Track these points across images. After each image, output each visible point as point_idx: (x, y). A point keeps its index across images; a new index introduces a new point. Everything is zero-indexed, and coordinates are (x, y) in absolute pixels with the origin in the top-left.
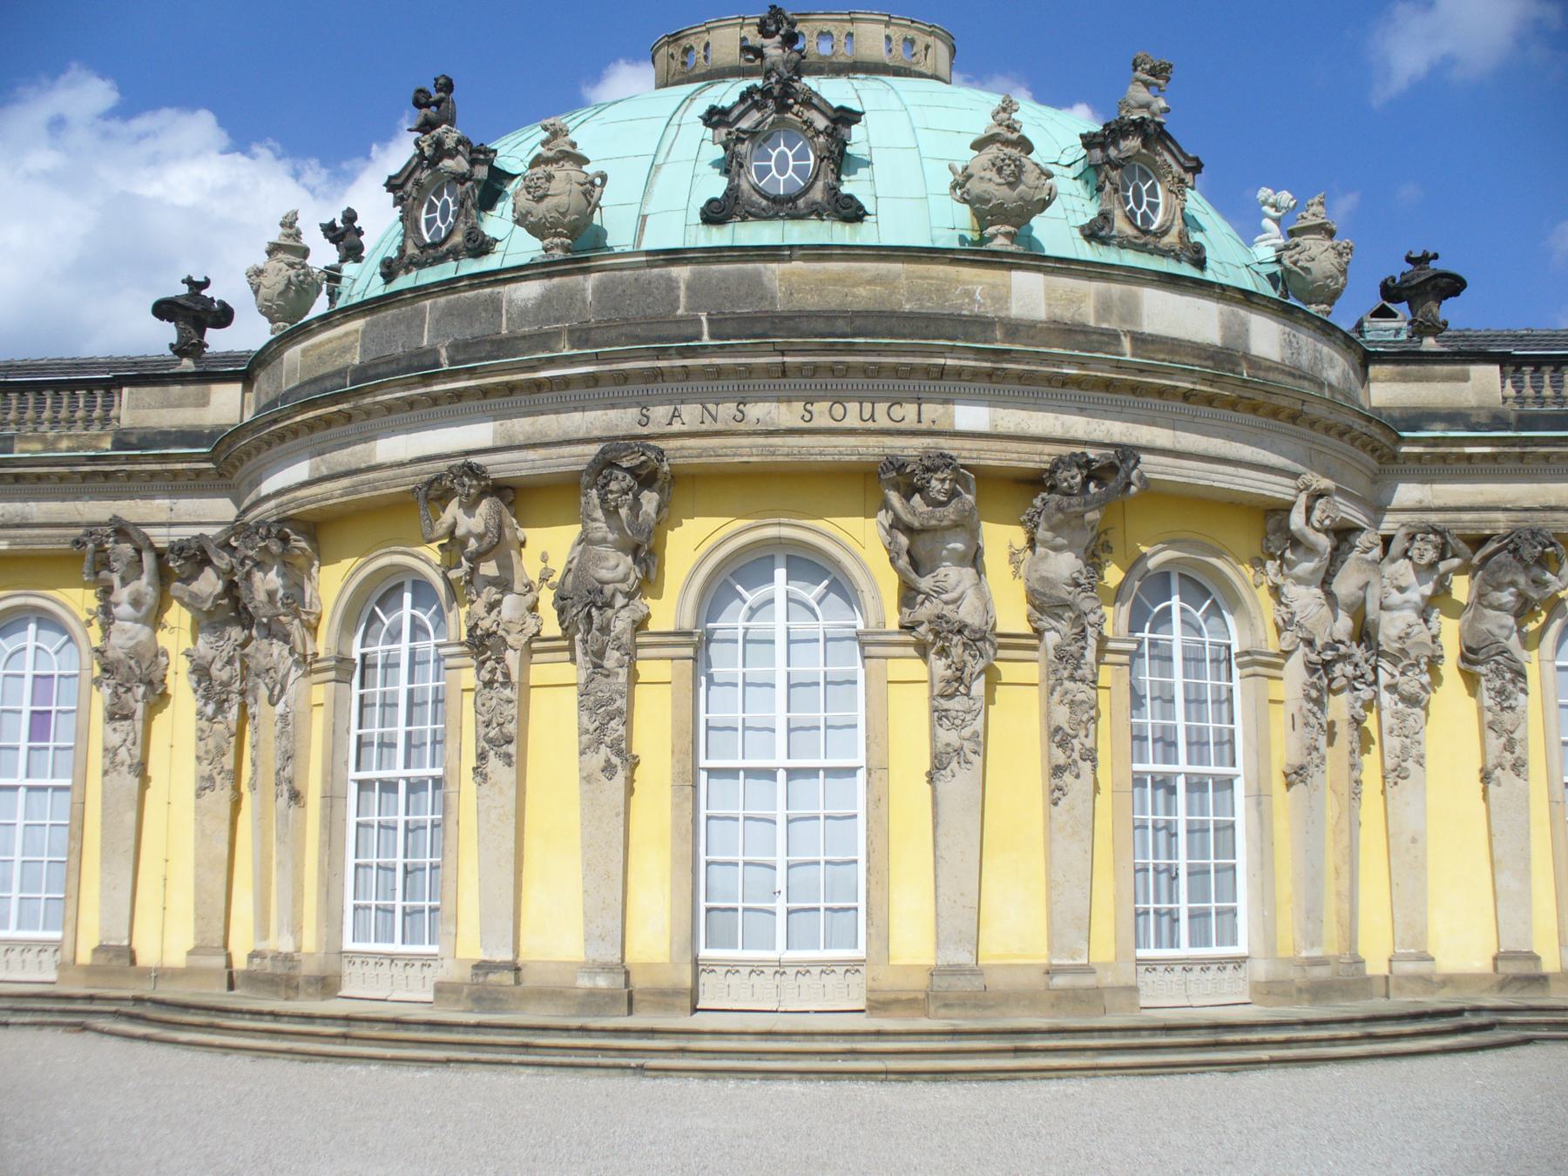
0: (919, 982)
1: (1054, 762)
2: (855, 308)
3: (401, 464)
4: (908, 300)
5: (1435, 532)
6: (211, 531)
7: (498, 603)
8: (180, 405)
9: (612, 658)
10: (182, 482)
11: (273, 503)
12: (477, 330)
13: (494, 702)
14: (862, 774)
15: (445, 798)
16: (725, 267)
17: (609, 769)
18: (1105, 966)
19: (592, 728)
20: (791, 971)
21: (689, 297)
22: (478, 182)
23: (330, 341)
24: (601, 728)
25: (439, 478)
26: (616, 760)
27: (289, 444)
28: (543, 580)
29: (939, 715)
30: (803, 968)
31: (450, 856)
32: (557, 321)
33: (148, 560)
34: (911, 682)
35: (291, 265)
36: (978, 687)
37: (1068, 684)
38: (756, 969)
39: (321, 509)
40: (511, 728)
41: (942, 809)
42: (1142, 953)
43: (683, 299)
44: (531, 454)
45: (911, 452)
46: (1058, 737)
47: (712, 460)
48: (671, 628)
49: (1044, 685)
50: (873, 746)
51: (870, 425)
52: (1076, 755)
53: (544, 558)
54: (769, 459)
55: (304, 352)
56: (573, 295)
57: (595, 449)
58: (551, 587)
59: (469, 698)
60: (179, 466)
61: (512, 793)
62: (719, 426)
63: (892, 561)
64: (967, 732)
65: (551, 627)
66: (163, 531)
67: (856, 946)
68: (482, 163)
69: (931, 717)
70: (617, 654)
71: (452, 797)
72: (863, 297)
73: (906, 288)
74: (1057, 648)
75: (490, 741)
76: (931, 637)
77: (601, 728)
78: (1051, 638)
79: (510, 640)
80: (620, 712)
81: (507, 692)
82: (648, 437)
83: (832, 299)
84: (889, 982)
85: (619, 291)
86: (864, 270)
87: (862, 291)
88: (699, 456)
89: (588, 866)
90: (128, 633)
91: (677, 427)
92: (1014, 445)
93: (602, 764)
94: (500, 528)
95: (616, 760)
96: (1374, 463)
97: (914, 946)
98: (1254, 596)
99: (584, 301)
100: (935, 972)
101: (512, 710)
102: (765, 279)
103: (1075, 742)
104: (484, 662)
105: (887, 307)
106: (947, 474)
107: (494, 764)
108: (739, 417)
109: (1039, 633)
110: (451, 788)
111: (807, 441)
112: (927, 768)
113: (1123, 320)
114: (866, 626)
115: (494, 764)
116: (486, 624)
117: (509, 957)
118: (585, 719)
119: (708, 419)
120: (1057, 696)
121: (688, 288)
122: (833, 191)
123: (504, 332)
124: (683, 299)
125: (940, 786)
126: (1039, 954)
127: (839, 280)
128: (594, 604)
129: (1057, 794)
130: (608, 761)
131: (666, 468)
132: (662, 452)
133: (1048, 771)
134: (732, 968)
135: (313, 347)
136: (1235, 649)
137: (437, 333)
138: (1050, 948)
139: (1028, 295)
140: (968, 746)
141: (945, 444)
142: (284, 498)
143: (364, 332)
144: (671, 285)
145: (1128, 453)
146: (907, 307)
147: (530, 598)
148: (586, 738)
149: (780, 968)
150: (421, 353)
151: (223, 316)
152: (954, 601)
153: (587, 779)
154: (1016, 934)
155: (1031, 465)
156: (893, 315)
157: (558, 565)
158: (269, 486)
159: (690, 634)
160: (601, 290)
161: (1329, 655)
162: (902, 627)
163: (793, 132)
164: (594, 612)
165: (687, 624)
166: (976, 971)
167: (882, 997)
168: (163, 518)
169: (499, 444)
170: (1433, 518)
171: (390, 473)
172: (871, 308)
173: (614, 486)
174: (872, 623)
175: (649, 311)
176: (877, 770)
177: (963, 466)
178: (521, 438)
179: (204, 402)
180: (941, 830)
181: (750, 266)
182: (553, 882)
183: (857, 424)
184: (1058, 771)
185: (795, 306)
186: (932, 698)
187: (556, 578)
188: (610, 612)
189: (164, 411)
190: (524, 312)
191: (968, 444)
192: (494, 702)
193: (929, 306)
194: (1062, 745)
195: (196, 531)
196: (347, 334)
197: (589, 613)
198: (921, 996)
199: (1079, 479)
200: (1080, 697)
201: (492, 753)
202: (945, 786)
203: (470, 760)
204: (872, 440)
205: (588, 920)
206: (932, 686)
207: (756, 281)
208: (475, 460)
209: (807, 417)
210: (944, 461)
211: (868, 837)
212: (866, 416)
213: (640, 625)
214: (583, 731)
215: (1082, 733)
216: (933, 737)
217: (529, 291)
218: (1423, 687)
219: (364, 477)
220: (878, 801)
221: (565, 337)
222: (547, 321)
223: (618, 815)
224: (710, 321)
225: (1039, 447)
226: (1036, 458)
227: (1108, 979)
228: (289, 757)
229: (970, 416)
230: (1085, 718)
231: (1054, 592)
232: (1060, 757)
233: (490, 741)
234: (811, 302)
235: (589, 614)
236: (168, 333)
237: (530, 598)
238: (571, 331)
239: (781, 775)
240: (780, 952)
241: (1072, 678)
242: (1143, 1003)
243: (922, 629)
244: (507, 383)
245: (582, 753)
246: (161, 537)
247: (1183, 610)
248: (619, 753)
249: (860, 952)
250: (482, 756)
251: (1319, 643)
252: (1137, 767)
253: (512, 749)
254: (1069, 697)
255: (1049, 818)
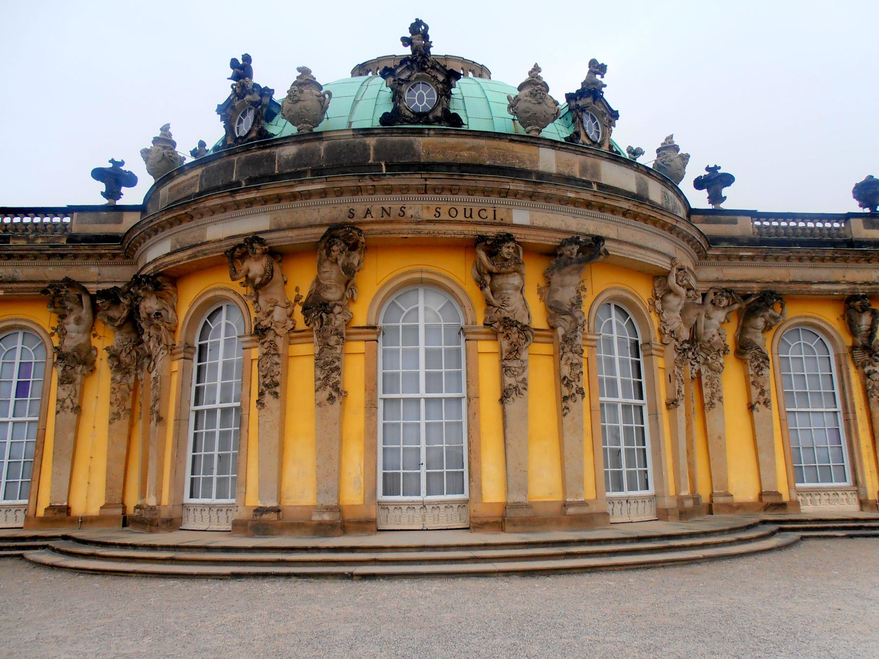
0: (497, 512)
1: (563, 394)
2: (461, 162)
3: (220, 241)
4: (489, 160)
5: (727, 291)
6: (120, 286)
7: (272, 311)
8: (105, 222)
9: (333, 340)
10: (105, 260)
11: (152, 267)
12: (262, 171)
13: (269, 365)
14: (464, 402)
15: (241, 419)
16: (394, 139)
17: (331, 398)
18: (591, 500)
19: (322, 377)
20: (429, 507)
21: (375, 154)
22: (264, 106)
23: (184, 182)
24: (327, 377)
25: (240, 246)
26: (334, 394)
27: (161, 235)
28: (296, 301)
29: (505, 370)
30: (436, 505)
31: (244, 450)
32: (305, 166)
33: (86, 300)
34: (487, 357)
35: (165, 148)
36: (524, 355)
37: (570, 355)
38: (411, 506)
39: (176, 268)
40: (277, 378)
41: (509, 420)
42: (609, 494)
43: (372, 155)
44: (290, 234)
45: (490, 234)
46: (566, 382)
47: (387, 236)
48: (364, 324)
49: (557, 357)
50: (471, 386)
51: (470, 219)
52: (574, 391)
53: (297, 289)
54: (418, 236)
55: (170, 189)
56: (314, 153)
57: (324, 230)
58: (300, 304)
59: (255, 364)
60: (103, 252)
61: (277, 413)
62: (391, 218)
63: (481, 288)
64: (520, 378)
65: (301, 325)
66: (94, 286)
67: (463, 493)
68: (268, 95)
69: (501, 371)
70: (336, 338)
71: (245, 417)
72: (465, 156)
73: (486, 152)
74: (564, 336)
75: (266, 386)
76: (501, 329)
77: (327, 377)
78: (560, 331)
79: (278, 331)
80: (338, 368)
81: (276, 359)
82: (354, 223)
83: (450, 157)
84: (482, 512)
85: (338, 150)
86: (466, 143)
87: (465, 154)
88: (381, 234)
89: (319, 452)
90: (75, 336)
91: (369, 218)
92: (541, 233)
93: (328, 396)
94: (272, 271)
95: (334, 394)
96: (696, 258)
97: (493, 492)
98: (650, 317)
99: (320, 156)
100: (506, 506)
101: (276, 369)
102: (415, 146)
103: (573, 384)
104: (263, 344)
105: (478, 162)
106: (511, 244)
107: (268, 398)
108: (402, 214)
109: (553, 328)
110: (245, 412)
111: (438, 227)
112: (498, 396)
113: (593, 176)
114: (466, 324)
115: (268, 398)
116: (266, 323)
117: (274, 504)
118: (318, 372)
119: (385, 215)
120: (563, 362)
121: (375, 149)
122: (446, 111)
123: (277, 172)
124: (372, 155)
125: (507, 407)
126: (558, 497)
127: (453, 148)
128: (324, 311)
129: (565, 411)
130: (331, 395)
131: (363, 240)
132: (361, 231)
133: (560, 400)
134: (398, 506)
135: (175, 186)
136: (640, 343)
137: (241, 173)
138: (564, 492)
139: (548, 161)
140: (521, 386)
141: (508, 230)
142: (158, 263)
143: (202, 176)
144: (366, 147)
145: (598, 240)
146: (488, 163)
147: (289, 310)
148: (318, 383)
149: (424, 505)
150: (231, 184)
151: (131, 180)
152: (513, 311)
153: (319, 405)
154: (544, 487)
155: (551, 243)
156: (480, 166)
157: (304, 293)
158: (151, 255)
159: (375, 328)
160: (330, 150)
161: (686, 346)
162: (485, 324)
163: (425, 81)
164: (323, 314)
165: (373, 324)
166: (528, 506)
167: (479, 521)
168: (95, 279)
169: (273, 228)
170: (724, 286)
171: (212, 246)
172: (470, 162)
173: (335, 248)
174: (470, 322)
175: (354, 161)
176: (473, 399)
177: (518, 243)
178: (285, 225)
179: (119, 221)
180: (507, 431)
181: (407, 139)
182: (300, 463)
183: (463, 219)
184: (565, 398)
185: (430, 160)
186: (502, 360)
187: (303, 300)
188: (331, 316)
189: (97, 226)
190: (287, 162)
191: (520, 231)
192: (269, 365)
193: (499, 163)
194: (567, 385)
195: (112, 286)
196: (192, 178)
197: (321, 317)
198: (500, 520)
199: (575, 250)
200: (575, 361)
201: (267, 392)
202: (511, 407)
203: (255, 396)
204: (471, 228)
205: (319, 482)
206: (502, 354)
207: (410, 147)
208: (261, 236)
209: (437, 215)
210: (509, 238)
211: (469, 434)
212: (468, 215)
213: (347, 323)
214: (317, 379)
215: (577, 380)
216: (502, 381)
217: (289, 151)
218: (721, 365)
219: (199, 249)
220: (473, 415)
221: (309, 173)
222: (299, 166)
223: (336, 424)
224: (386, 165)
225: (555, 235)
226: (552, 240)
227: (594, 509)
228: (157, 400)
229: (520, 216)
230: (578, 372)
231: (562, 308)
232: (566, 392)
233: (266, 386)
234: (439, 158)
235: (321, 317)
236: (102, 187)
237: (289, 310)
238: (312, 171)
239: (423, 402)
240: (423, 497)
241: (571, 351)
242: (612, 520)
243: (496, 325)
244: (278, 195)
245: (316, 391)
246: (93, 288)
247: (617, 323)
248: (337, 390)
249: (465, 496)
250: (261, 394)
251: (681, 340)
252: (601, 399)
253: (278, 389)
254: (569, 362)
255: (560, 425)
